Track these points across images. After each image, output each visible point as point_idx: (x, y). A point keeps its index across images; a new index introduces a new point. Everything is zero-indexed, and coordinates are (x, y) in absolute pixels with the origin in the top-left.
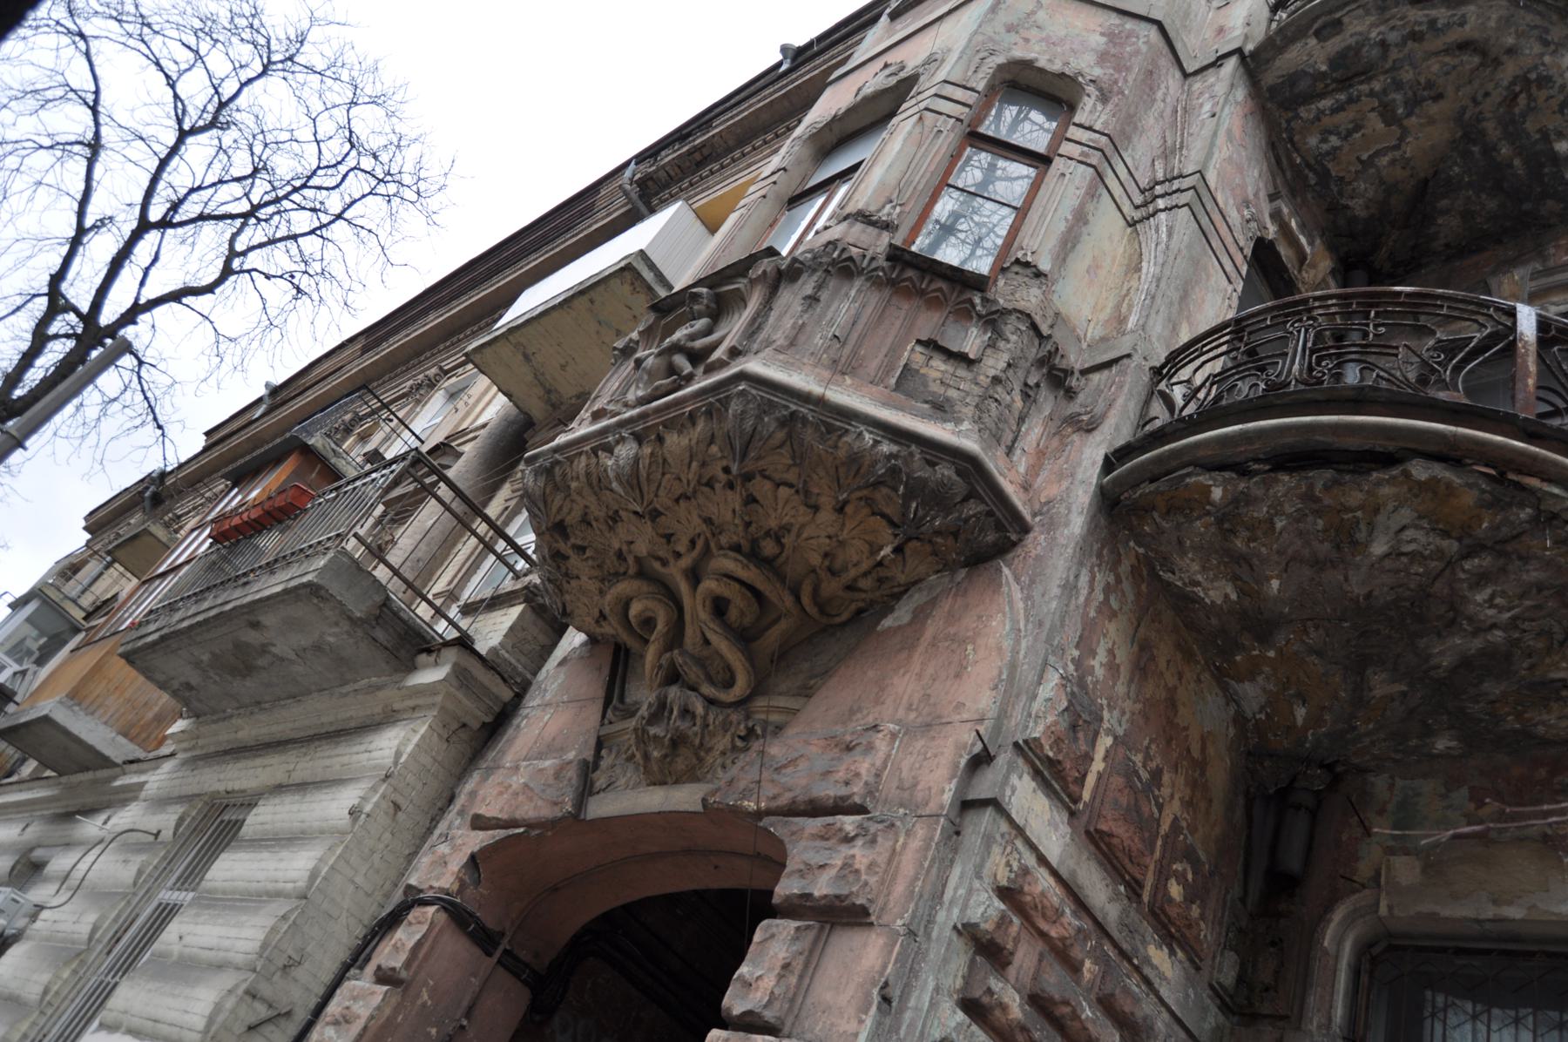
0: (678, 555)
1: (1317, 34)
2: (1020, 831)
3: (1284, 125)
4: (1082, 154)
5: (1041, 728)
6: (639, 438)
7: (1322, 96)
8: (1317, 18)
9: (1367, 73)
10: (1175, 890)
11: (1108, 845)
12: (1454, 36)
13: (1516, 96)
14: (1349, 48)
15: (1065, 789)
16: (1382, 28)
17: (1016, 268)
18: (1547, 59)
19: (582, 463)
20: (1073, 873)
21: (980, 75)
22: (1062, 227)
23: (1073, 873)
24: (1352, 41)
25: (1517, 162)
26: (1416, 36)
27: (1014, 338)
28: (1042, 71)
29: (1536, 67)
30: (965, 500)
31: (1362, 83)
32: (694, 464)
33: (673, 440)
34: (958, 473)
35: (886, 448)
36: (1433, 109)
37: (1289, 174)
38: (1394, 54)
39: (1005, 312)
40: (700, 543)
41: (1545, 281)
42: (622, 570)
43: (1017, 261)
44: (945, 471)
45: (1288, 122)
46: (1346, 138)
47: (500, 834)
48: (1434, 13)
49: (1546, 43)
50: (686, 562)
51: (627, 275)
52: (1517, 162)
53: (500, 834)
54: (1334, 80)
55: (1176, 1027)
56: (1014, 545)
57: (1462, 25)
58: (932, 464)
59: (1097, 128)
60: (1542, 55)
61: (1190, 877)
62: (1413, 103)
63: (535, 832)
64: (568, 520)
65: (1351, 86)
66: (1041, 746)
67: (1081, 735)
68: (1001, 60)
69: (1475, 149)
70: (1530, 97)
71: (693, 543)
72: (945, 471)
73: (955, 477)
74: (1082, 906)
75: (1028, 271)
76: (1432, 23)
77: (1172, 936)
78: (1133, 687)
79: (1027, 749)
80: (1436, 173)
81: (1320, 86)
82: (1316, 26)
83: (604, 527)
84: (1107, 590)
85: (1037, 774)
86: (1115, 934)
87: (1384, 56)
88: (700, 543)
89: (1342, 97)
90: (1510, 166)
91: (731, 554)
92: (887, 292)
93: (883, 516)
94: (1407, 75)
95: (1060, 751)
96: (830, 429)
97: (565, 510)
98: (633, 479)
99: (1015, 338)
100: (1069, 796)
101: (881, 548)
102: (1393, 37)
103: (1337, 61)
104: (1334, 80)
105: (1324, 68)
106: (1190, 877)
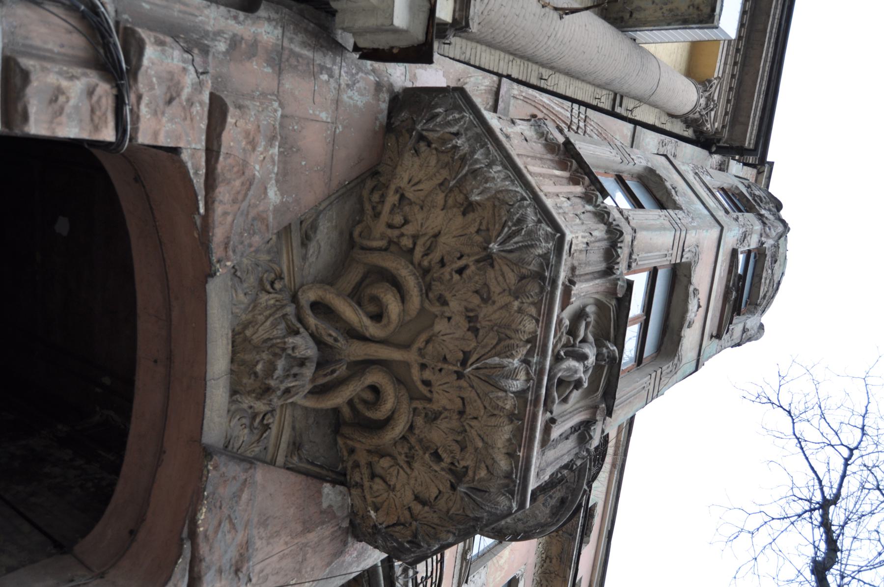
0: (423, 366)
6: (521, 394)
19: (529, 326)
32: (480, 444)
33: (504, 434)
40: (424, 390)
42: (431, 295)
47: (199, 183)
49: (519, 520)
50: (415, 372)
51: (706, 10)
53: (199, 183)
63: (198, 221)
64: (491, 274)
71: (427, 383)
83: (470, 306)
88: (424, 390)
91: (408, 425)
93: (394, 525)
97: (500, 279)
98: (493, 379)
101: (376, 510)
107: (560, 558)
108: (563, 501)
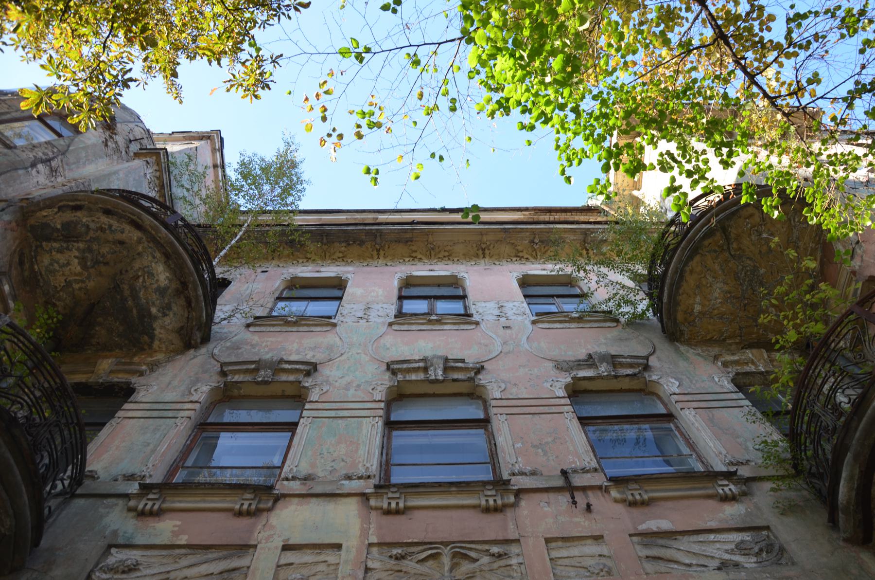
3: (34, 248)
7: (55, 240)
8: (61, 201)
9: (77, 238)
12: (119, 236)
13: (138, 277)
14: (72, 221)
16: (89, 219)
18: (153, 264)
24: (75, 219)
25: (135, 311)
26: (102, 229)
29: (148, 267)
31: (75, 242)
36: (103, 269)
37: (26, 273)
38: (91, 234)
41: (121, 367)
45: (37, 247)
46: (61, 267)
48: (112, 222)
52: (135, 311)
54: (62, 235)
57: (122, 233)
60: (151, 262)
62: (97, 262)
65: (69, 241)
69: (118, 297)
70: (144, 281)
76: (110, 226)
80: (99, 302)
81: (56, 235)
82: (61, 204)
87: (87, 233)
89: (65, 245)
94: (95, 247)
102: (92, 225)
103: (66, 225)
104: (62, 235)
105: (59, 227)
107: (408, 241)
108: (107, 212)
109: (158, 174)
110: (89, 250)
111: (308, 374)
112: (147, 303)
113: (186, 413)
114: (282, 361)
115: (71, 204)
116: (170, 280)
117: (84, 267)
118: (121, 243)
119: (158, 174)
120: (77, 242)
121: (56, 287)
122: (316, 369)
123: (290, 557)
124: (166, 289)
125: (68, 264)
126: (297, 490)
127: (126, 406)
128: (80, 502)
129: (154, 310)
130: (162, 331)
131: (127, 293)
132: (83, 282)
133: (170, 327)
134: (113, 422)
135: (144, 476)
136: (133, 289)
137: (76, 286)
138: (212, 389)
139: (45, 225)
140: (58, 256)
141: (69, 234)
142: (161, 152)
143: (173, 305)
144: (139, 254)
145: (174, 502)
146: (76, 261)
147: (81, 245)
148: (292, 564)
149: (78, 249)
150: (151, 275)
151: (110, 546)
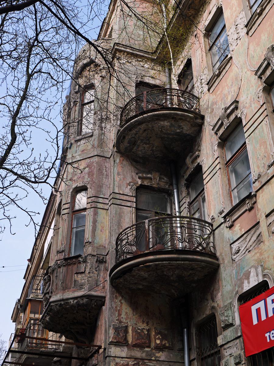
1: (122, 142)
2: (115, 357)
4: (91, 205)
5: (111, 339)
7: (134, 148)
8: (119, 141)
10: (158, 342)
11: (138, 345)
15: (123, 343)
17: (86, 244)
20: (131, 355)
21: (69, 198)
22: (91, 228)
23: (131, 355)
27: (89, 261)
28: (79, 187)
30: (91, 301)
34: (87, 299)
35: (76, 301)
39: (86, 257)
43: (86, 243)
44: (85, 300)
52: (175, 136)
55: (170, 363)
56: (105, 301)
58: (83, 300)
59: (92, 196)
60: (158, 125)
61: (161, 337)
66: (113, 341)
67: (121, 333)
68: (71, 190)
70: (164, 130)
72: (85, 300)
73: (87, 300)
74: (136, 359)
75: (88, 243)
77: (162, 349)
78: (134, 314)
79: (111, 343)
84: (120, 301)
85: (115, 345)
86: (146, 358)
89: (137, 146)
90: (174, 137)
92: (67, 266)
94: (141, 138)
95: (117, 339)
96: (66, 303)
99: (90, 260)
100: (124, 344)
102: (133, 136)
103: (129, 142)
106: (161, 337)
109: (126, 54)
110: (142, 140)
111: (236, 108)
112: (174, 131)
113: (218, 167)
114: (226, 109)
115: (121, 139)
116: (169, 122)
117: (148, 144)
118: (145, 130)
119: (126, 54)
120: (137, 142)
121: (151, 154)
122: (238, 102)
123: (270, 219)
124: (171, 124)
125: (145, 148)
126: (258, 186)
127: (204, 176)
128: (216, 232)
129: (178, 131)
130: (189, 131)
131: (166, 136)
132: (154, 146)
133: (188, 129)
134: (205, 187)
135: (223, 210)
136: (165, 134)
137: (154, 148)
138: (218, 145)
139: (126, 148)
140: (140, 149)
141: (133, 143)
142: (116, 47)
143: (180, 124)
144: (152, 127)
145: (234, 217)
146: (144, 145)
147: (139, 142)
148: (271, 223)
149: (140, 143)
150: (163, 127)
151: (231, 245)
